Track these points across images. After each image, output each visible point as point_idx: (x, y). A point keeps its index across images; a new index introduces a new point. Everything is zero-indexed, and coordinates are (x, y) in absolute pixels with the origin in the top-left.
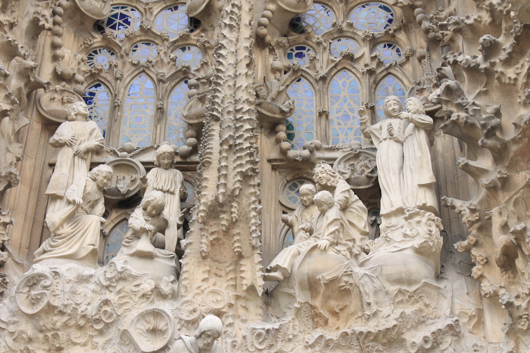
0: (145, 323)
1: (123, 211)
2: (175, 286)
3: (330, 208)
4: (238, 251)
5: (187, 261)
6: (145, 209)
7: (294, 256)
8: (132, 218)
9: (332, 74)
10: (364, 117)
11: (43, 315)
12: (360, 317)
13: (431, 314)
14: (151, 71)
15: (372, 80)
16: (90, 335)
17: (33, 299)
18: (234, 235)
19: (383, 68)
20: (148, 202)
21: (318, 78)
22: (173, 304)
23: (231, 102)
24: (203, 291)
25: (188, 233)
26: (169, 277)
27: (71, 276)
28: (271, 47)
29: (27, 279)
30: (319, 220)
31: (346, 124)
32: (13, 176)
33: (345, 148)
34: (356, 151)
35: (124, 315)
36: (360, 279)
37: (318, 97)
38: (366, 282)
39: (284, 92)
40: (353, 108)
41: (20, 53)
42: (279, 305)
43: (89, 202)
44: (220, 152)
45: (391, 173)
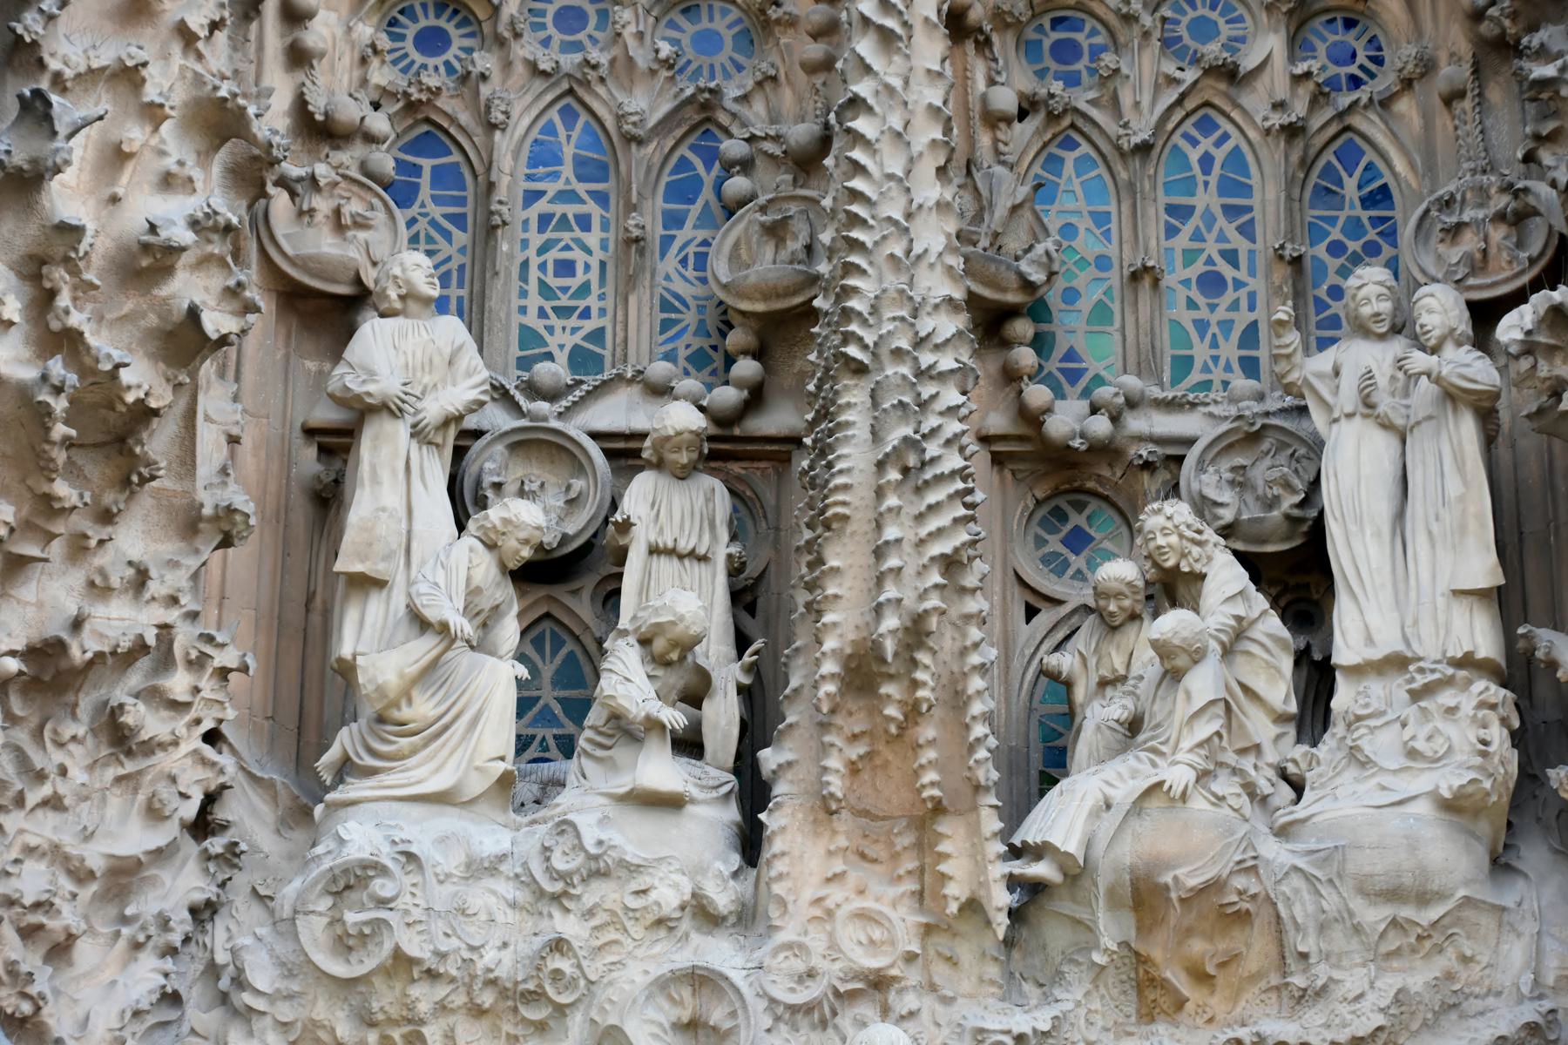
0: (666, 1005)
1: (541, 592)
2: (744, 887)
3: (1196, 662)
4: (932, 798)
5: (783, 822)
6: (645, 642)
7: (1095, 814)
8: (614, 677)
9: (1170, 126)
10: (1287, 340)
11: (379, 982)
12: (1277, 988)
13: (1476, 984)
14: (597, 96)
15: (1295, 157)
16: (508, 1034)
17: (349, 935)
18: (920, 746)
19: (1328, 113)
20: (658, 625)
21: (1126, 146)
22: (742, 947)
23: (903, 319)
24: (830, 913)
25: (780, 732)
26: (725, 862)
27: (452, 862)
28: (981, 38)
29: (330, 875)
30: (1160, 693)
31: (1213, 307)
32: (238, 518)
33: (1216, 402)
34: (1253, 424)
35: (605, 980)
36: (1279, 882)
37: (1126, 207)
38: (1297, 891)
39: (1027, 205)
40: (1235, 251)
41: (255, 136)
42: (1044, 947)
43: (478, 614)
44: (880, 493)
45: (1368, 532)
